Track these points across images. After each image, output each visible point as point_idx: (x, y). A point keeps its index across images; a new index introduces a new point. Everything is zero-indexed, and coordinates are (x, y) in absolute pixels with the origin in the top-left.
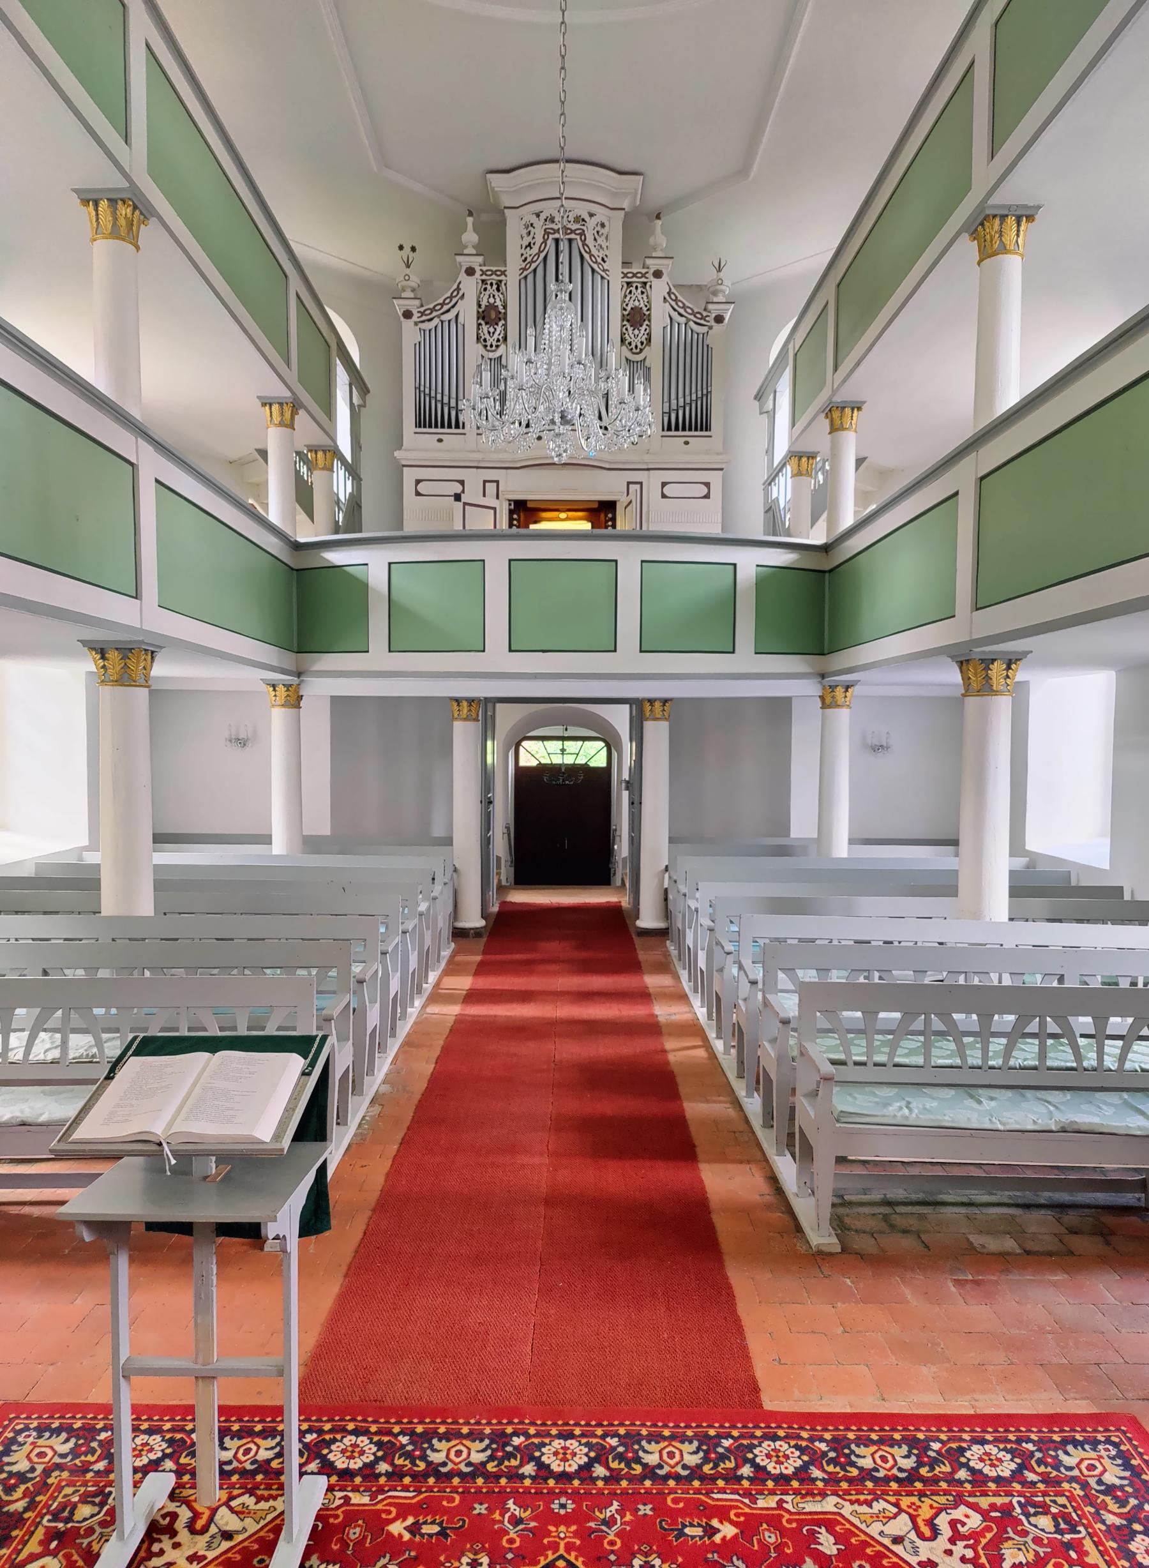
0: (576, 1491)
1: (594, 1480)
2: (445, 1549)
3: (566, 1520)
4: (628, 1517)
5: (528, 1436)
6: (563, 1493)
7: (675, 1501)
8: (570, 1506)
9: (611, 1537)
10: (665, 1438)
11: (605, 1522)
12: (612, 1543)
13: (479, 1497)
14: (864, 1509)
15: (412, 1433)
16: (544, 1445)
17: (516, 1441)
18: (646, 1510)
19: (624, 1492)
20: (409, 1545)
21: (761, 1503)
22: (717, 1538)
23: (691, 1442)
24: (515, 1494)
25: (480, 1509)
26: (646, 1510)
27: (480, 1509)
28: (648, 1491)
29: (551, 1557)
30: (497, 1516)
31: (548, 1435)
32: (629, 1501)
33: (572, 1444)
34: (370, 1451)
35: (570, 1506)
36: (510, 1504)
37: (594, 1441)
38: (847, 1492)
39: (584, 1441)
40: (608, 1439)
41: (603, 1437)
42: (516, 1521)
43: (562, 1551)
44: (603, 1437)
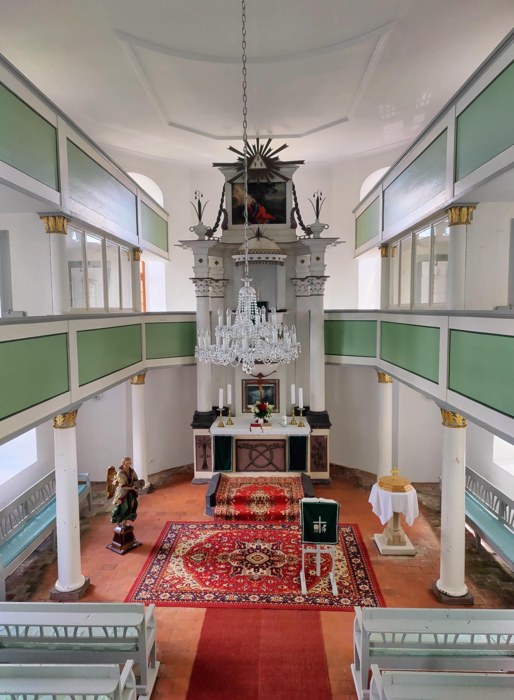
0: (252, 592)
1: (248, 594)
2: (276, 584)
3: (254, 588)
4: (242, 588)
5: (262, 602)
6: (254, 592)
7: (233, 590)
8: (253, 590)
9: (246, 585)
10: (232, 601)
11: (247, 587)
12: (246, 584)
13: (271, 592)
14: (197, 588)
15: (288, 603)
16: (259, 600)
17: (264, 601)
18: (239, 589)
19: (243, 592)
20: (283, 585)
21: (216, 590)
22: (227, 584)
23: (226, 600)
24: (264, 592)
25: (271, 590)
26: (239, 589)
27: (271, 590)
28: (238, 592)
29: (257, 582)
30: (267, 589)
31: (258, 602)
32: (242, 590)
33: (252, 600)
34: (296, 599)
35: (253, 590)
36: (265, 590)
37: (247, 601)
38: (199, 591)
39: (250, 601)
40: (244, 601)
41: (245, 602)
42: (264, 588)
43: (255, 583)
44: (245, 602)
